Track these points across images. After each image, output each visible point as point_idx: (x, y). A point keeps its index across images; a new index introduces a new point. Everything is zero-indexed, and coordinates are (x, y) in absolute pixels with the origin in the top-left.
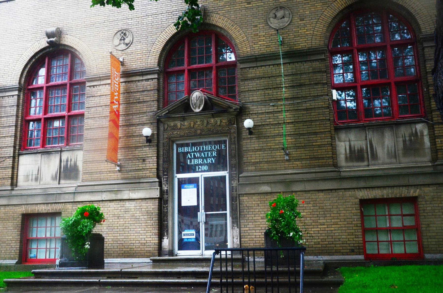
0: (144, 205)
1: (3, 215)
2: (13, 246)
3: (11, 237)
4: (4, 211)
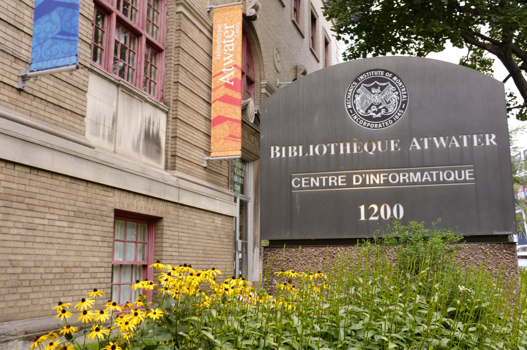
0: (226, 223)
1: (84, 204)
2: (102, 280)
3: (97, 259)
4: (85, 194)
